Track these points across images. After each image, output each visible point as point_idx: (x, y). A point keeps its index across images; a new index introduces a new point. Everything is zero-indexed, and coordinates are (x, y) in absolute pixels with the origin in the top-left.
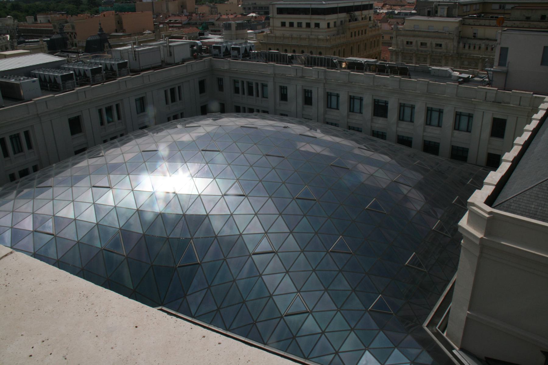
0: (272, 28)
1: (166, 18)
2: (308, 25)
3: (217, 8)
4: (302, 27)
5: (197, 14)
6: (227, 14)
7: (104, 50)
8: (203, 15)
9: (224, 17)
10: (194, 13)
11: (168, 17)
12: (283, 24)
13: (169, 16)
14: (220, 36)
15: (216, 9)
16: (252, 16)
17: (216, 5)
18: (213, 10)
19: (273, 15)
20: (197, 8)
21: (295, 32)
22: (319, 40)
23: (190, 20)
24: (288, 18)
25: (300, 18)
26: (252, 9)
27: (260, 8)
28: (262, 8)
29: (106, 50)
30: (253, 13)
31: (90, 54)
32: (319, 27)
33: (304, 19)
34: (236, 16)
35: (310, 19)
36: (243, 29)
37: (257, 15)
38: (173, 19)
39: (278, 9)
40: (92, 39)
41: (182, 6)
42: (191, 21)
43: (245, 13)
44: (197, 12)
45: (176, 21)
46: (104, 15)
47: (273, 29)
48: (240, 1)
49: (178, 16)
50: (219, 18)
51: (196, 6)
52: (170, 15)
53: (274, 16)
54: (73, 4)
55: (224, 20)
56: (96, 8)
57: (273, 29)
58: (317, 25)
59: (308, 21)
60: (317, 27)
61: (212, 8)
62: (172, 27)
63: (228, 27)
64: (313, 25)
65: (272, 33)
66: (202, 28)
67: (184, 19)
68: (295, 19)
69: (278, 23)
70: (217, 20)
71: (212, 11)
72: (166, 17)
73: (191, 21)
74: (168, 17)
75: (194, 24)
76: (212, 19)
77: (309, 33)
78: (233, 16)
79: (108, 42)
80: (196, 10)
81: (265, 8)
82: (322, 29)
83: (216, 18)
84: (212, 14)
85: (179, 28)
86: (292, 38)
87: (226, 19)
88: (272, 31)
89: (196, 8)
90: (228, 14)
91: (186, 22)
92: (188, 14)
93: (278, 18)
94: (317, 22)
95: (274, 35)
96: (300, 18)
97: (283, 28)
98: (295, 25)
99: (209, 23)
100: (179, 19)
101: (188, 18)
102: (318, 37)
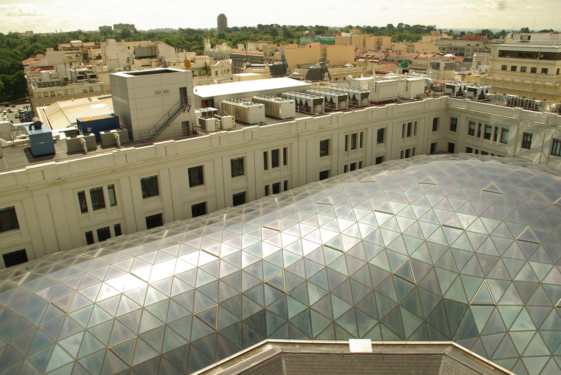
0: (491, 71)
1: (363, 53)
2: (534, 70)
3: (414, 46)
4: (526, 72)
5: (393, 51)
6: (425, 53)
7: (323, 79)
8: (399, 52)
9: (422, 55)
10: (390, 50)
11: (365, 52)
12: (504, 68)
13: (366, 52)
14: (425, 75)
15: (413, 48)
16: (451, 57)
17: (412, 43)
18: (410, 48)
19: (493, 58)
20: (394, 45)
21: (517, 77)
22: (545, 87)
23: (387, 56)
24: (510, 62)
25: (525, 63)
26: (446, 49)
27: (455, 49)
28: (457, 49)
29: (325, 79)
30: (448, 53)
31: (311, 82)
32: (546, 73)
33: (529, 63)
34: (434, 56)
35: (538, 63)
36: (451, 70)
37: (455, 56)
38: (370, 54)
39: (500, 51)
40: (314, 67)
41: (377, 42)
42: (388, 58)
43: (441, 54)
44: (393, 49)
45: (373, 56)
46: (310, 46)
47: (492, 72)
48: (433, 41)
49: (375, 51)
50: (417, 57)
51: (393, 44)
52: (368, 50)
53: (494, 59)
54: (270, 35)
55: (422, 59)
56: (290, 40)
57: (492, 72)
58: (545, 71)
59: (534, 66)
60: (544, 72)
61: (409, 46)
62: (372, 62)
63: (436, 66)
64: (539, 71)
65: (489, 76)
66: (401, 65)
67: (380, 55)
68: (519, 63)
69: (499, 66)
70: (414, 59)
71: (408, 49)
72: (363, 52)
73: (388, 58)
74: (365, 52)
75: (391, 61)
76: (410, 56)
77: (533, 79)
78: (431, 56)
79: (328, 72)
80: (393, 47)
81: (461, 49)
82: (550, 75)
83: (415, 57)
84: (408, 52)
85: (378, 63)
86: (514, 83)
87: (425, 58)
88: (490, 74)
89: (392, 45)
90: (427, 54)
91: (383, 58)
92: (385, 51)
93: (499, 61)
94: (545, 67)
95: (493, 79)
96: (525, 63)
97: (504, 72)
98: (518, 69)
99: (407, 60)
100: (377, 55)
101: (385, 54)
102: (545, 84)
